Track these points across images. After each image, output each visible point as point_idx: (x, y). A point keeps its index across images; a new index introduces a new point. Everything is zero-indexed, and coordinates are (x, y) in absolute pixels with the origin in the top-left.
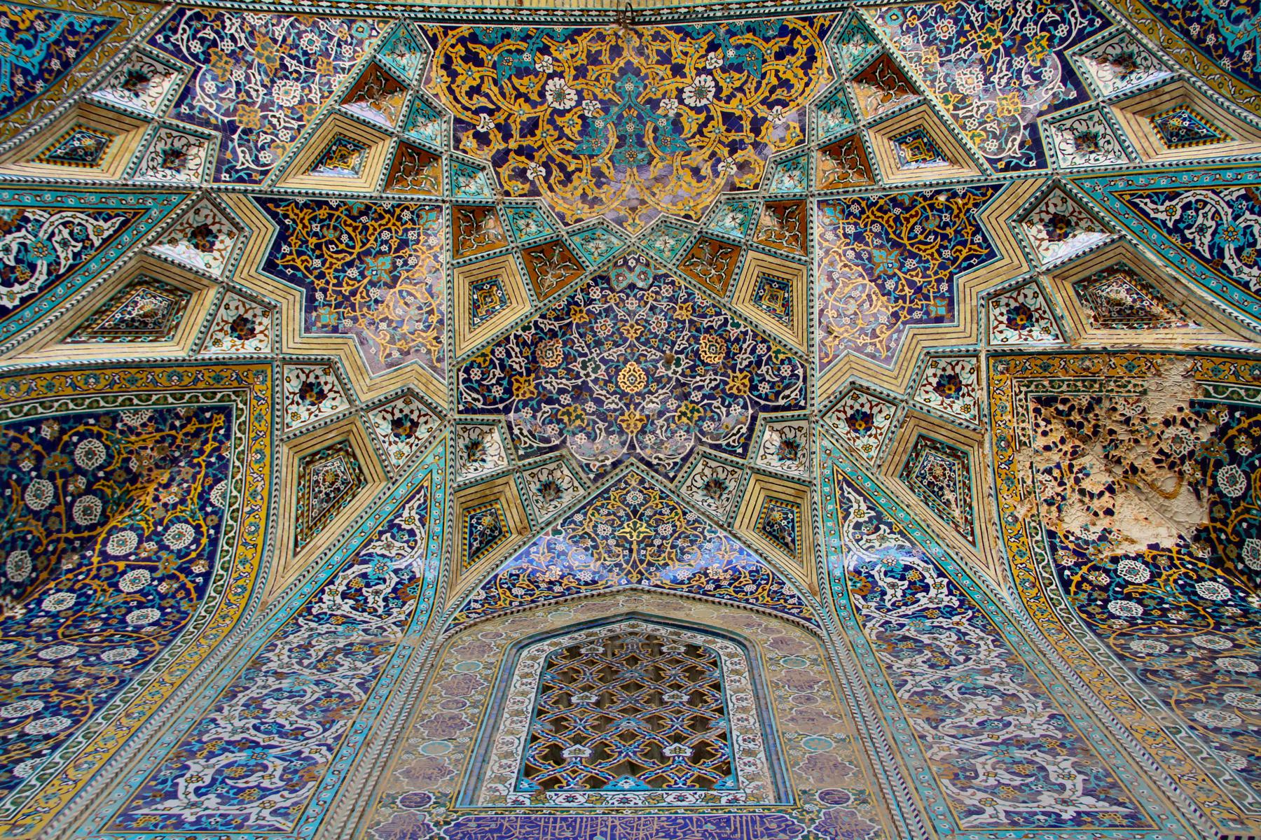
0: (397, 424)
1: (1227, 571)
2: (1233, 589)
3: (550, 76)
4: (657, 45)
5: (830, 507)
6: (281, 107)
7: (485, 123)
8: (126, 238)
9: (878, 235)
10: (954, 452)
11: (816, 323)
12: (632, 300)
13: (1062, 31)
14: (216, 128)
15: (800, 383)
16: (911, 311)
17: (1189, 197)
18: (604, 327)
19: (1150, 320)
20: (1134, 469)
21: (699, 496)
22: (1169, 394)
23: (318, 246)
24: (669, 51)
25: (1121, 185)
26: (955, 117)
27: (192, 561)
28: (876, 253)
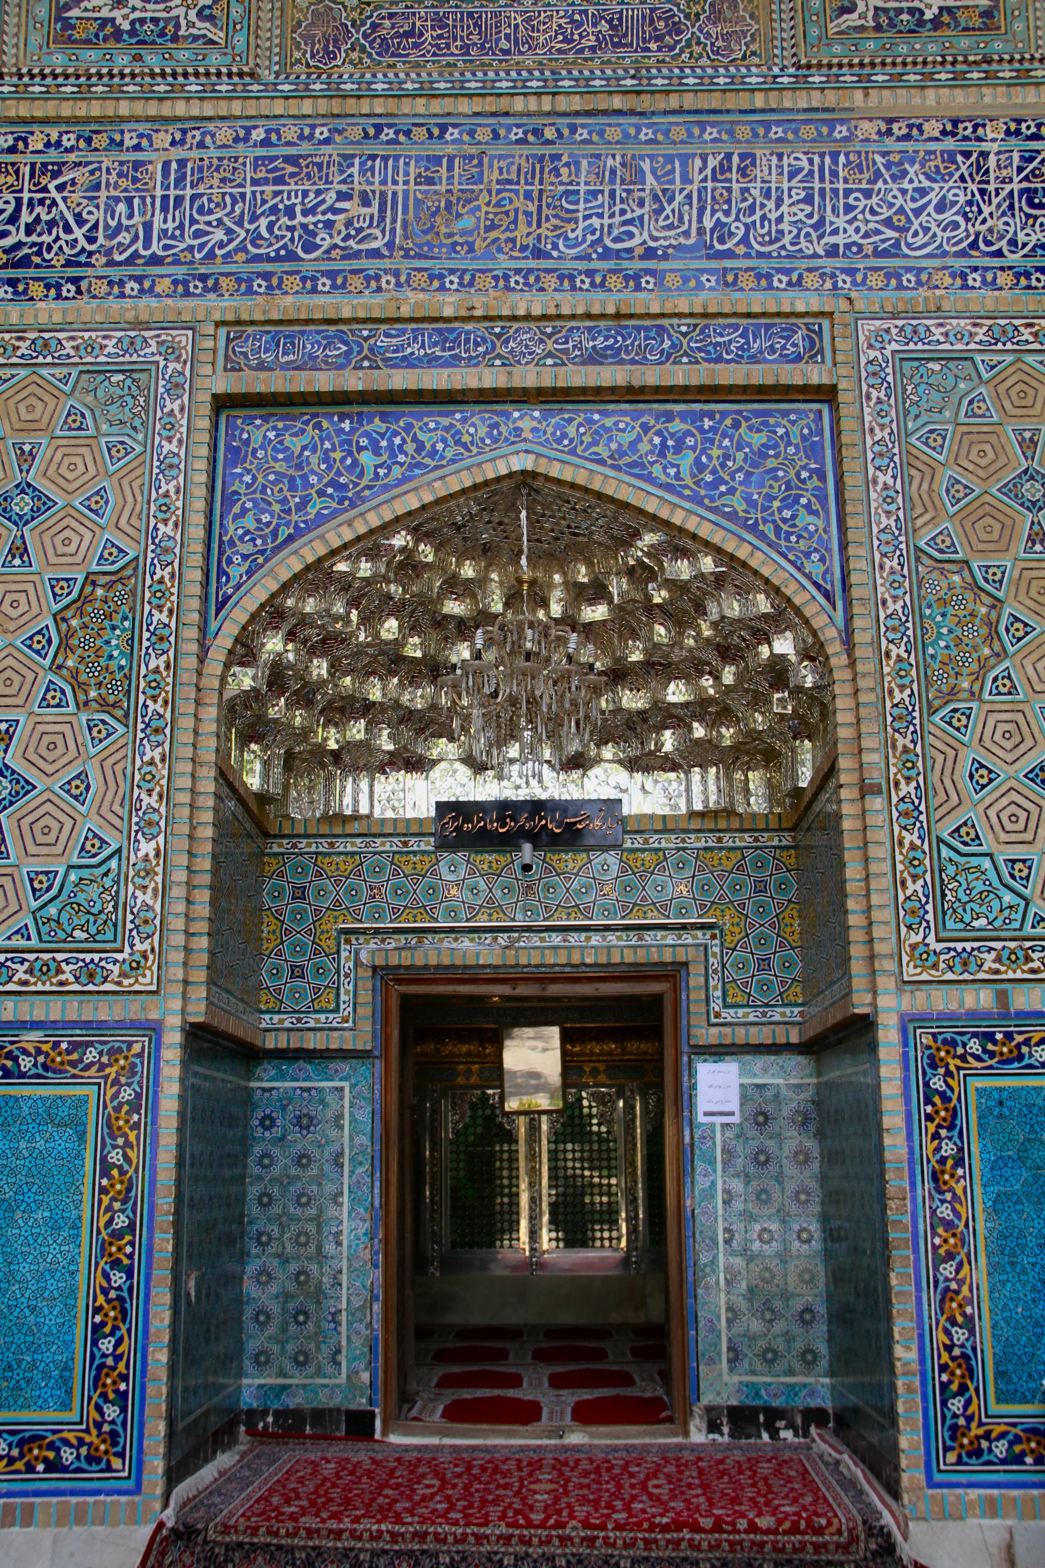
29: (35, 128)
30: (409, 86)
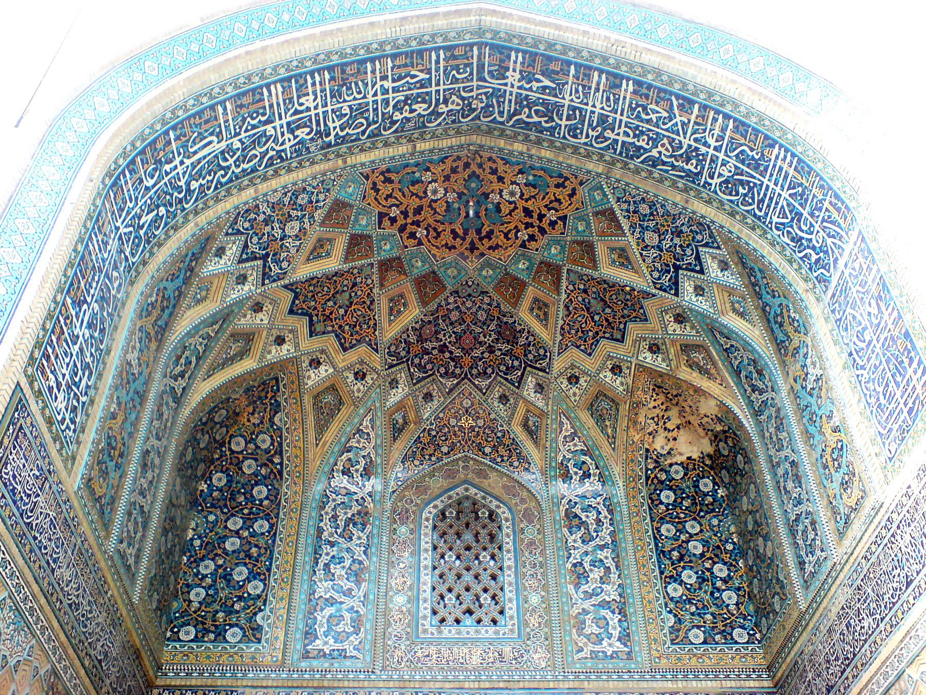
0: (356, 374)
1: (715, 473)
2: (715, 483)
3: (430, 183)
4: (490, 164)
5: (554, 426)
6: (290, 236)
7: (394, 212)
8: (225, 326)
9: (594, 293)
10: (613, 401)
11: (558, 332)
12: (469, 302)
13: (699, 237)
14: (260, 259)
15: (548, 360)
16: (604, 333)
17: (734, 343)
18: (455, 316)
19: (710, 377)
20: (690, 423)
21: (496, 404)
22: (709, 408)
23: (313, 296)
24: (496, 168)
25: (708, 321)
26: (641, 254)
27: (272, 456)
28: (592, 301)
29: (293, 690)
30: (428, 677)
